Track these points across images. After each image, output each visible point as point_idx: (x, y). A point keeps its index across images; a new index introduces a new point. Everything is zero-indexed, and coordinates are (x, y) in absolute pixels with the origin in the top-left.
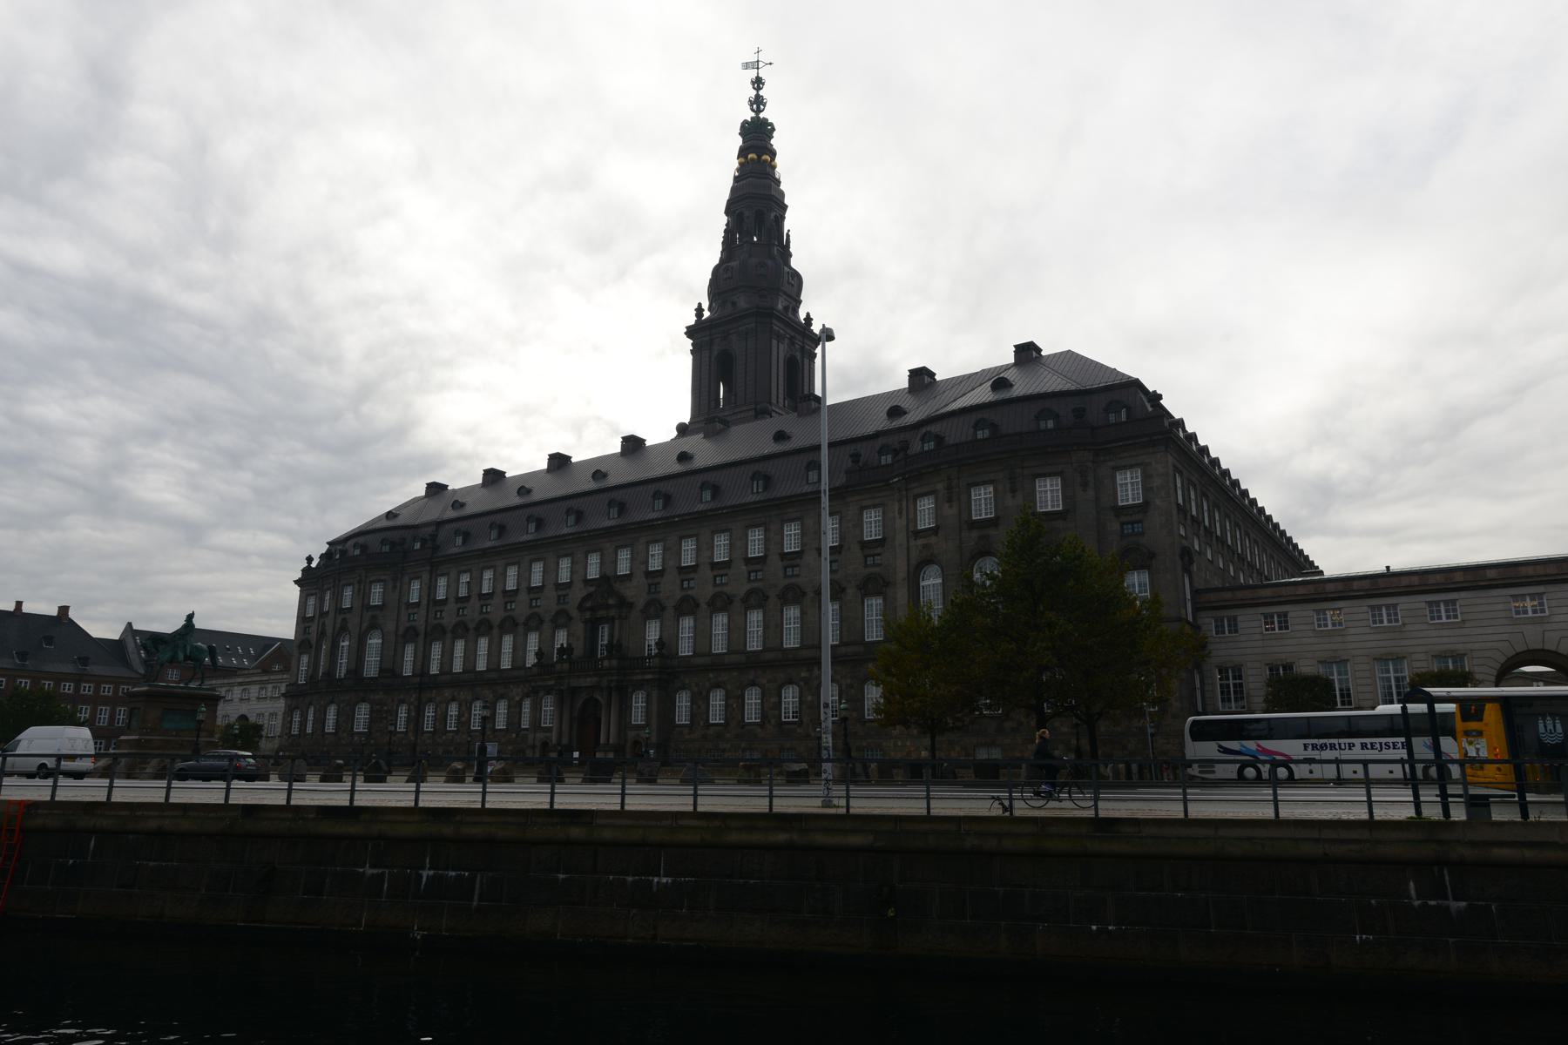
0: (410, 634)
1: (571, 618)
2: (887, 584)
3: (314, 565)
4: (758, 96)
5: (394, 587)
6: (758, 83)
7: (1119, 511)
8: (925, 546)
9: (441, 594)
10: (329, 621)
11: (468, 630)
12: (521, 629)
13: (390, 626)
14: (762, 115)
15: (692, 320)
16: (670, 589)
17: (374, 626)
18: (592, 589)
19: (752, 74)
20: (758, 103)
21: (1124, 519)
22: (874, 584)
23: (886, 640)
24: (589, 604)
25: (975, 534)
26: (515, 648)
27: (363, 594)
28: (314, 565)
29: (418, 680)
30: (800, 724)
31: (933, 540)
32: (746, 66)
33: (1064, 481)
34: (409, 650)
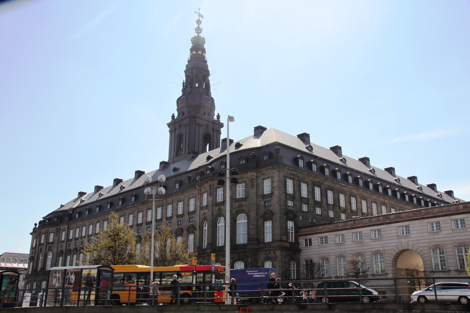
3: (37, 227)
5: (57, 235)
6: (199, 22)
7: (264, 196)
9: (71, 237)
10: (44, 248)
13: (55, 251)
14: (200, 35)
15: (170, 120)
17: (50, 249)
20: (198, 30)
21: (265, 200)
23: (194, 252)
25: (217, 208)
27: (47, 238)
28: (37, 227)
33: (246, 184)
34: (61, 258)
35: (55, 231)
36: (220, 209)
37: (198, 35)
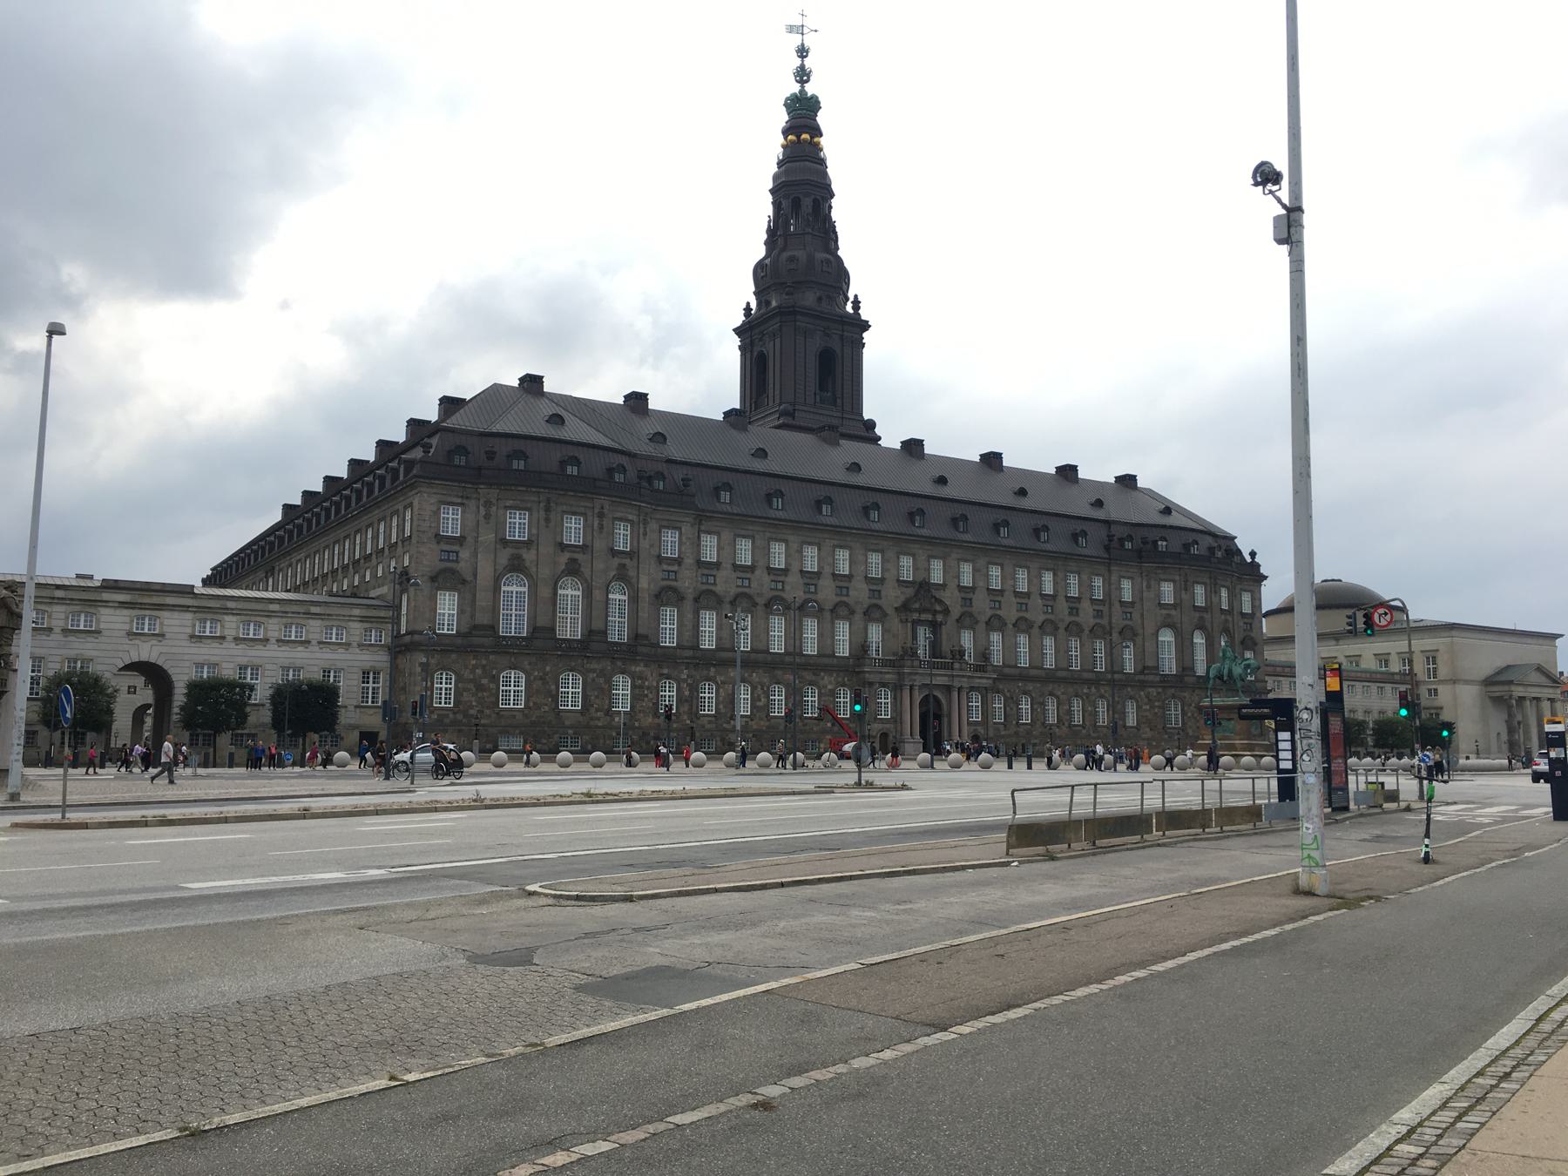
0: (667, 595)
1: (886, 615)
2: (1135, 635)
4: (802, 67)
7: (1243, 615)
8: (1169, 615)
11: (755, 605)
12: (827, 615)
16: (981, 604)
18: (910, 592)
19: (796, 40)
22: (1129, 633)
24: (917, 606)
26: (820, 635)
29: (689, 653)
30: (1083, 726)
31: (1173, 612)
32: (791, 29)
35: (635, 518)
36: (1201, 618)
37: (802, 91)
